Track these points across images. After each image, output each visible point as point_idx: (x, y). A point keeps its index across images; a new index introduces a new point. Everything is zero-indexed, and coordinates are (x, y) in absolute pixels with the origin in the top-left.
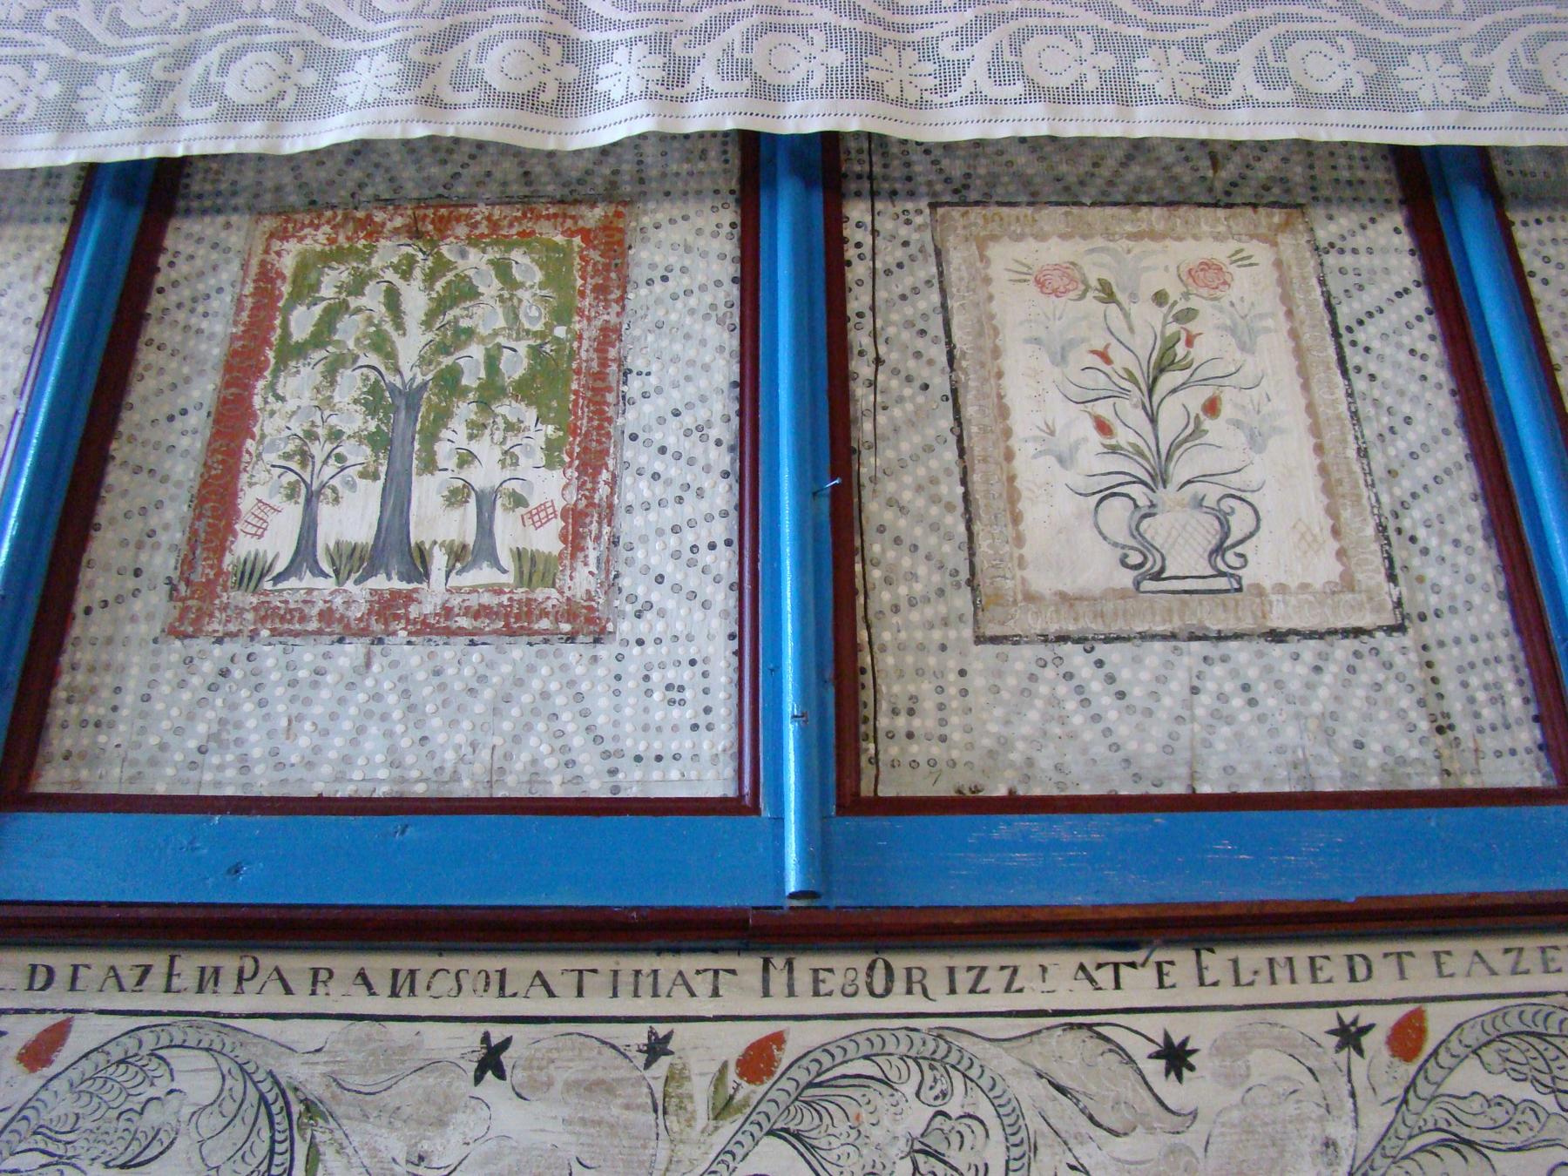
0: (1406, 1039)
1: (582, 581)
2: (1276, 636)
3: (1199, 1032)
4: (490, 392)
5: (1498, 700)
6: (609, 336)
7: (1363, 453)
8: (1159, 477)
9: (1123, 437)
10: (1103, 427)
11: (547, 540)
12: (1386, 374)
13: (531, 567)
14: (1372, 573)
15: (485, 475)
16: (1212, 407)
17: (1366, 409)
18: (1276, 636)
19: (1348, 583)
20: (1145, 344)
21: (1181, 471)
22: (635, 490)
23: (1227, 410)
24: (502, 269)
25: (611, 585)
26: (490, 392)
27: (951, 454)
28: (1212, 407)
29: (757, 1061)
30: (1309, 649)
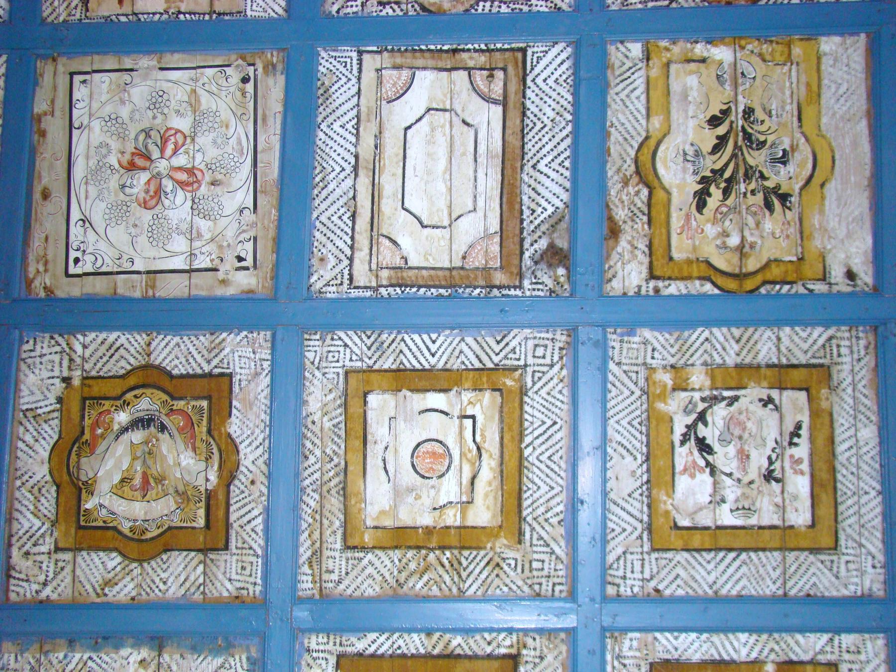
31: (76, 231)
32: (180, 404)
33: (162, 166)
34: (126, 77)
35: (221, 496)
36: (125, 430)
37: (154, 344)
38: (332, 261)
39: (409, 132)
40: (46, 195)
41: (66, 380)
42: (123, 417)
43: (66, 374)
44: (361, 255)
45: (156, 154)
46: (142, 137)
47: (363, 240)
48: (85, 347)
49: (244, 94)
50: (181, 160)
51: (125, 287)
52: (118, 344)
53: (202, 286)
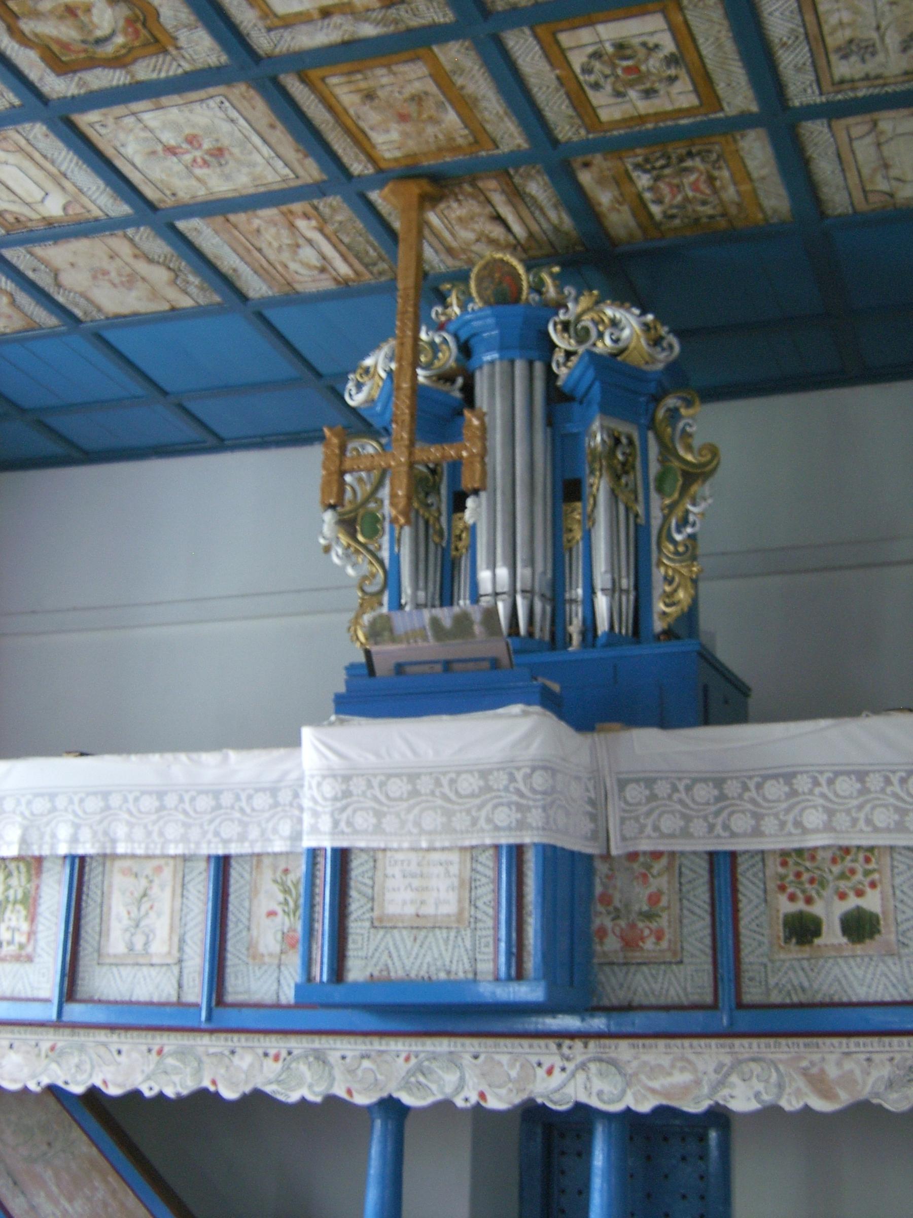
0: (160, 1052)
1: (29, 949)
2: (152, 965)
3: (124, 1048)
4: (15, 902)
5: (194, 980)
6: (38, 887)
7: (181, 919)
8: (137, 926)
9: (133, 915)
10: (129, 913)
11: (23, 939)
12: (191, 897)
13: (22, 946)
14: (175, 952)
15: (14, 923)
16: (151, 907)
17: (184, 908)
18: (152, 965)
19: (169, 953)
20: (141, 891)
21: (143, 924)
22: (40, 927)
23: (155, 908)
24: (18, 868)
25: (34, 949)
26: (15, 902)
27: (98, 920)
28: (151, 907)
29: (53, 1048)
30: (157, 968)
31: (234, 114)
32: (82, 55)
33: (198, 154)
34: (258, 182)
35: (9, 20)
36: (113, 34)
37: (129, 77)
38: (39, 136)
39: (43, 194)
40: (272, 126)
41: (178, 48)
42: (120, 40)
43: (183, 52)
44: (23, 142)
45: (207, 157)
46: (223, 162)
47: (29, 149)
48: (179, 65)
49: (169, 189)
50: (188, 158)
51: (176, 99)
52: (156, 72)
53: (119, 110)
